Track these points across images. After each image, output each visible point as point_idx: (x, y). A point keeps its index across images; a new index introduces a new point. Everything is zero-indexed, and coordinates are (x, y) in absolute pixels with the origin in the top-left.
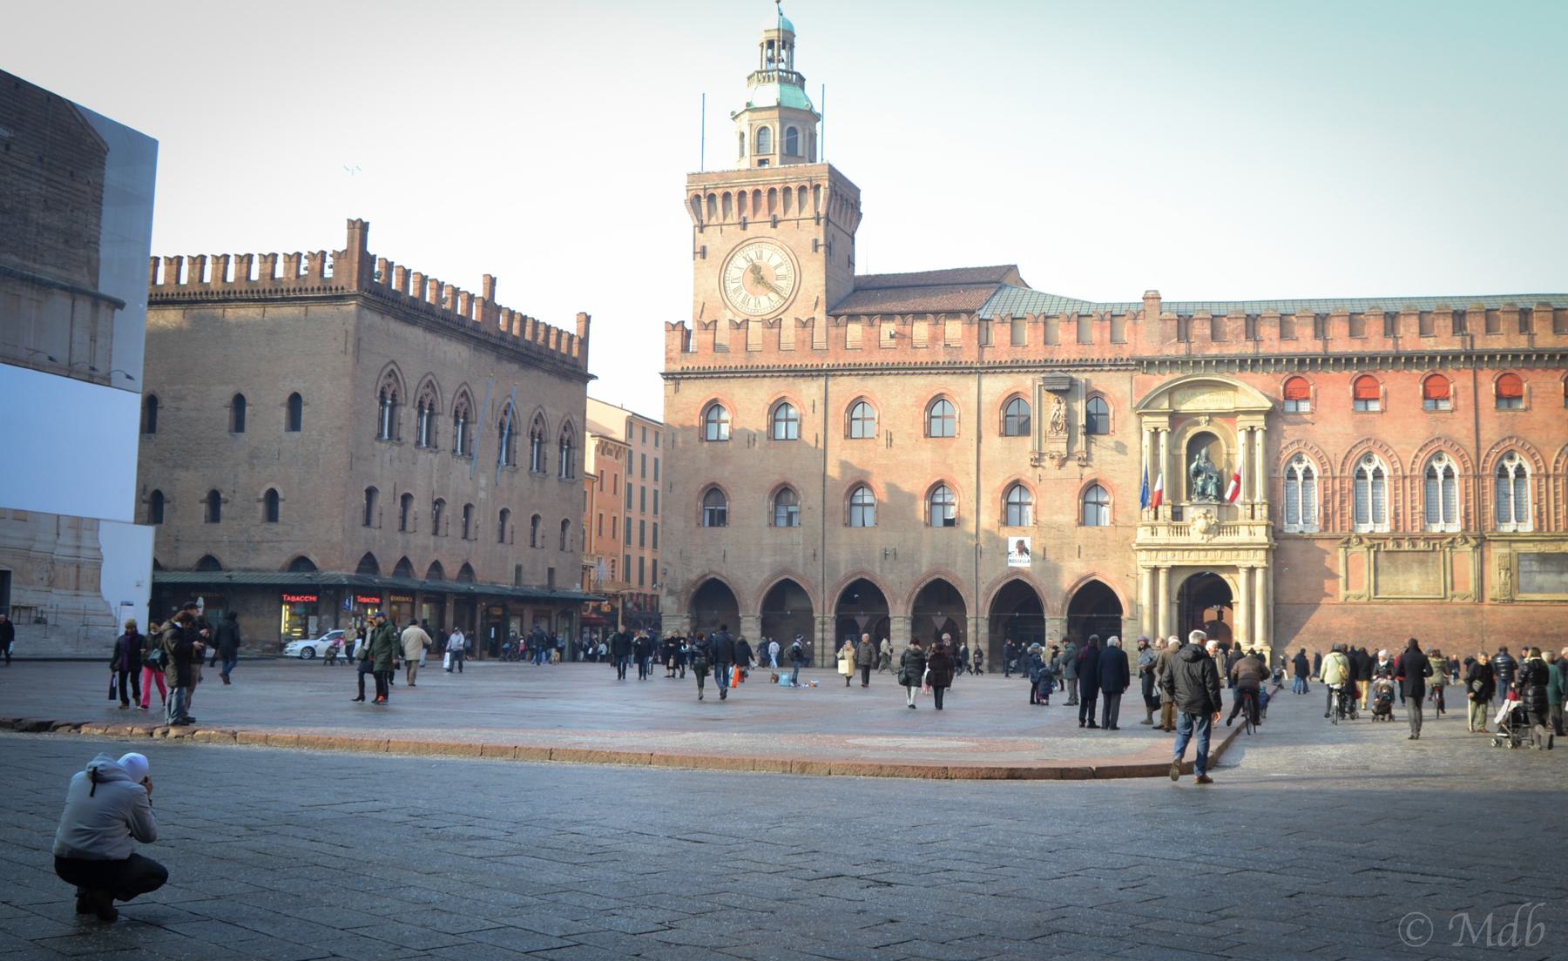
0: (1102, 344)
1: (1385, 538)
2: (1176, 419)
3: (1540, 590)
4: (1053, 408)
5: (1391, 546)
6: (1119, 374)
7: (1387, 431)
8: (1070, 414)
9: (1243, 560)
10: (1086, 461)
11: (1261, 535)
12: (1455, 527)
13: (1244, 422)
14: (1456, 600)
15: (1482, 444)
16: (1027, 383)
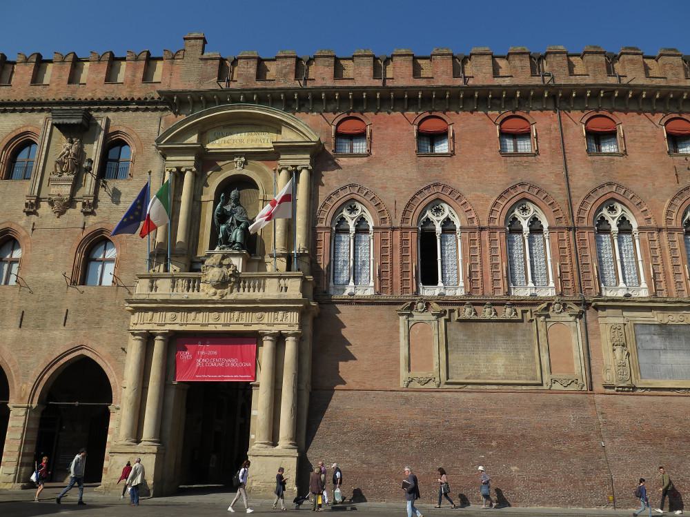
0: (133, 82)
1: (460, 303)
2: (207, 162)
3: (671, 374)
4: (62, 145)
5: (467, 312)
6: (148, 114)
7: (457, 176)
8: (80, 154)
9: (269, 323)
10: (91, 208)
11: (294, 289)
12: (549, 292)
13: (287, 160)
14: (557, 386)
15: (574, 193)
16: (38, 122)
